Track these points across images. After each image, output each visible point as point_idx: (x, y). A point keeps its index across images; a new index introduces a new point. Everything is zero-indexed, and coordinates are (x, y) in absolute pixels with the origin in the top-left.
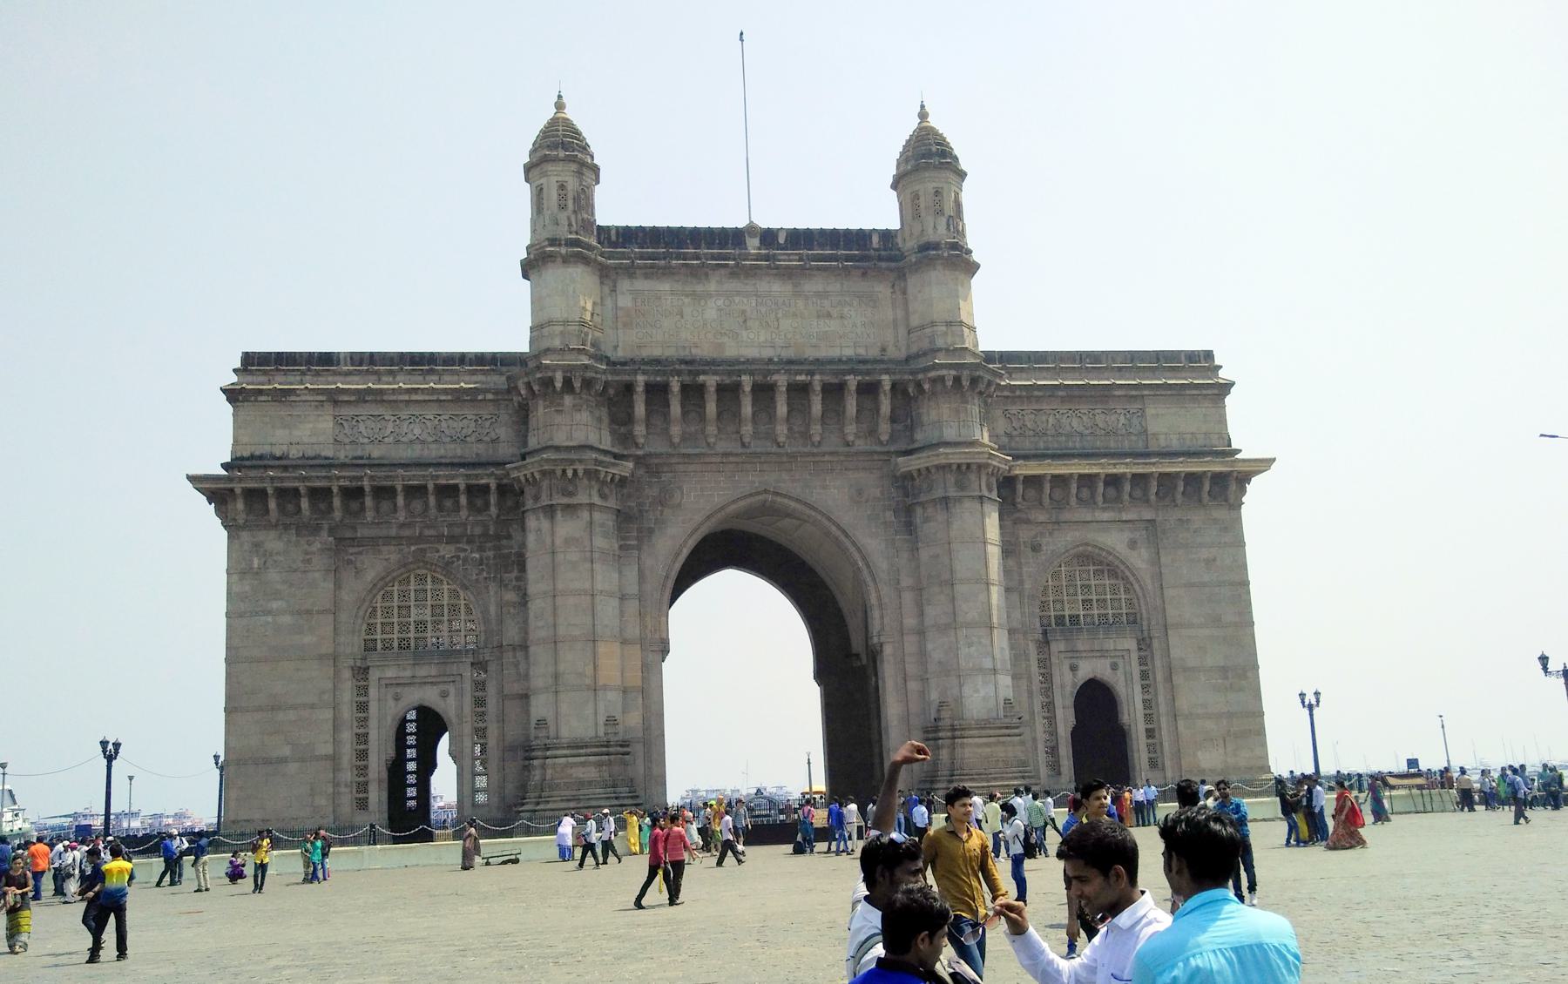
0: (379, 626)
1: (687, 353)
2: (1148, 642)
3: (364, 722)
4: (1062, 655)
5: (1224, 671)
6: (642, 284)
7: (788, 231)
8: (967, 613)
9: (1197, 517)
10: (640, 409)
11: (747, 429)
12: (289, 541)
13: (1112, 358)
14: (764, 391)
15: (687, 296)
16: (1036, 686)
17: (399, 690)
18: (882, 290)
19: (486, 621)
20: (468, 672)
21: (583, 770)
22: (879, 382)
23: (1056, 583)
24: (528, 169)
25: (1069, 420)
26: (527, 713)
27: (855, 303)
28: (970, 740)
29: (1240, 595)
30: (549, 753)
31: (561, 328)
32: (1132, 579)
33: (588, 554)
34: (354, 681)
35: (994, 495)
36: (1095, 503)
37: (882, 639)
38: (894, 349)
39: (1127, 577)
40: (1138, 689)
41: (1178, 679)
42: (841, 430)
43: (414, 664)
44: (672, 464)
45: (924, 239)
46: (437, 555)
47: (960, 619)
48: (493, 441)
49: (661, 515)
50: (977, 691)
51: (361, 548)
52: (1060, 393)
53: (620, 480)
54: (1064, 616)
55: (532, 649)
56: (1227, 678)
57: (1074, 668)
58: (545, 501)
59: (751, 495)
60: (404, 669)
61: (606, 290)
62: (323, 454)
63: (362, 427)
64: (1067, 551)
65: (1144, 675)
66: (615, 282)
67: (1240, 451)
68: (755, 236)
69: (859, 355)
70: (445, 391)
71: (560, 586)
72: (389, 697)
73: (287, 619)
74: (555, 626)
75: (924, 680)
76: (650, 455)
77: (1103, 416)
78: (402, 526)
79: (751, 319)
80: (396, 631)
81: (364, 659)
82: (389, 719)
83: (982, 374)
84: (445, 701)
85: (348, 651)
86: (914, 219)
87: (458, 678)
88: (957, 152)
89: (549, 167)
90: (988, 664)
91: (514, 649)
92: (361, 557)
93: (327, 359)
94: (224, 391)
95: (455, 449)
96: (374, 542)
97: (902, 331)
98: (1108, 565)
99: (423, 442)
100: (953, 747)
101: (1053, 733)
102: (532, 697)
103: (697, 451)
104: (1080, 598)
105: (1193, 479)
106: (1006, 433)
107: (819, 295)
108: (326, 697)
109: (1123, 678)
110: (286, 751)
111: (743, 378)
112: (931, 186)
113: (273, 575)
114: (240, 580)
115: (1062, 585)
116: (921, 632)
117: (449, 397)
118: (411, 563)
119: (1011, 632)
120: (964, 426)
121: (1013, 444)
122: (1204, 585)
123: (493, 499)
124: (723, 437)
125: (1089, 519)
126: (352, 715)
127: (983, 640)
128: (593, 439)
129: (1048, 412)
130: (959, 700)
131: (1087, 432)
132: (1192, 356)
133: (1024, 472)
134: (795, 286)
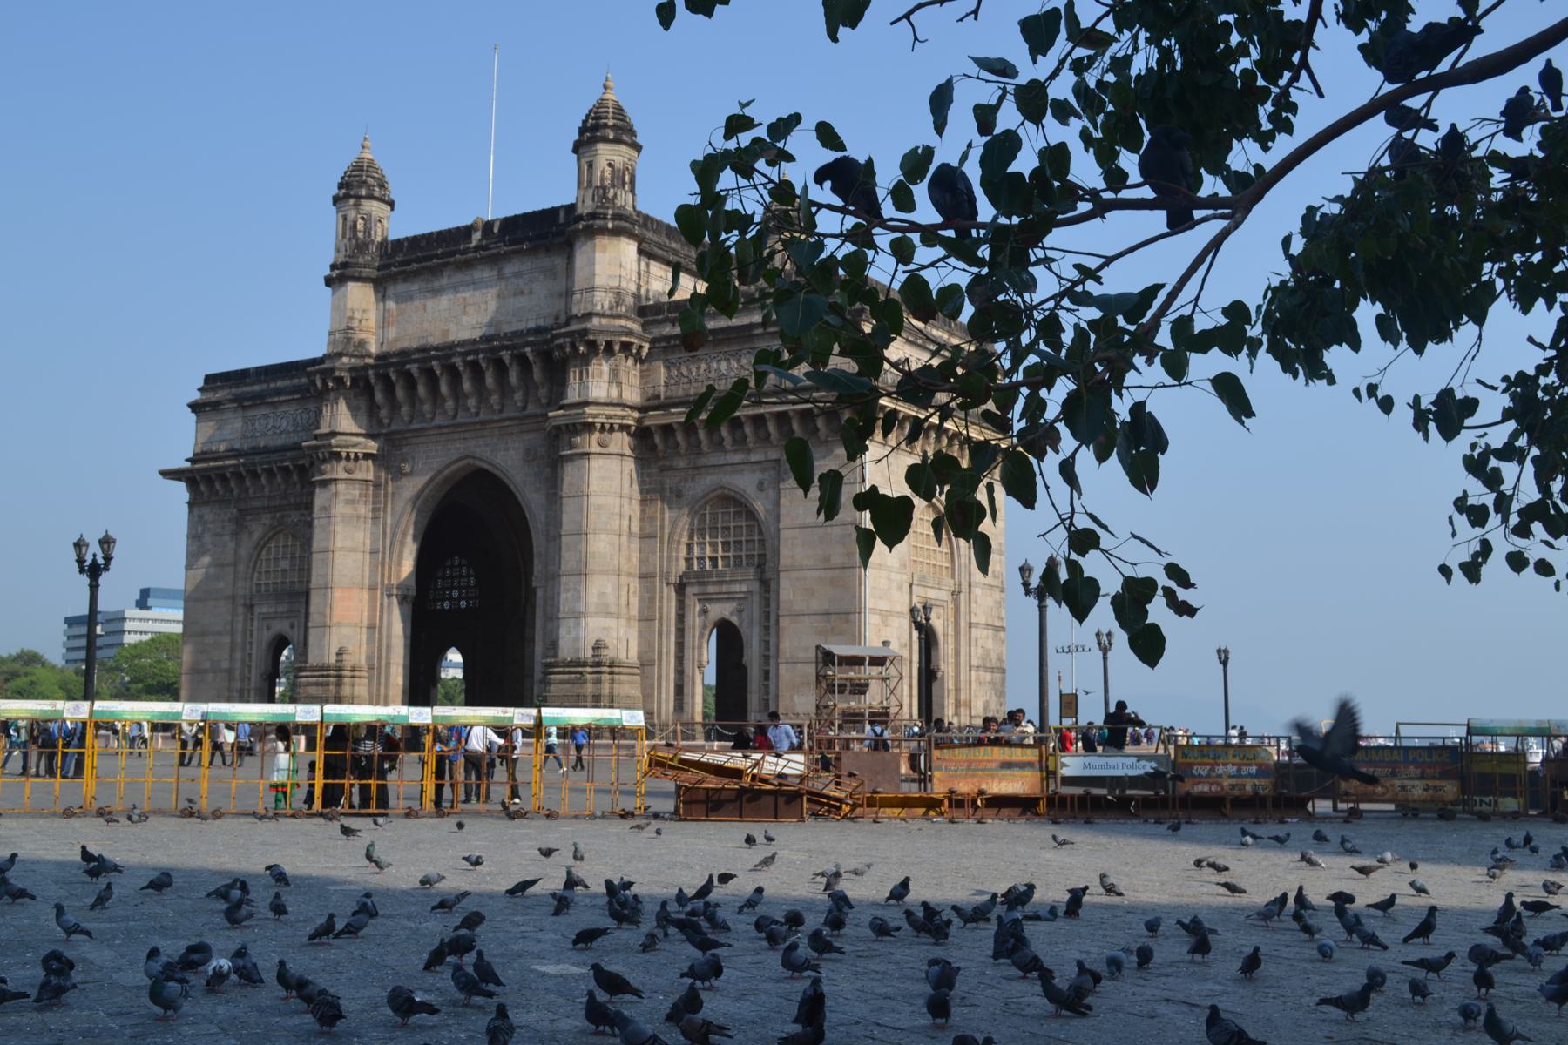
1: (422, 342)
10: (379, 397)
18: (559, 262)
21: (314, 688)
22: (524, 354)
27: (541, 278)
56: (829, 621)
57: (704, 612)
59: (457, 461)
61: (380, 295)
64: (707, 495)
76: (398, 432)
82: (264, 645)
110: (207, 665)
113: (207, 539)
121: (669, 393)
134: (500, 270)
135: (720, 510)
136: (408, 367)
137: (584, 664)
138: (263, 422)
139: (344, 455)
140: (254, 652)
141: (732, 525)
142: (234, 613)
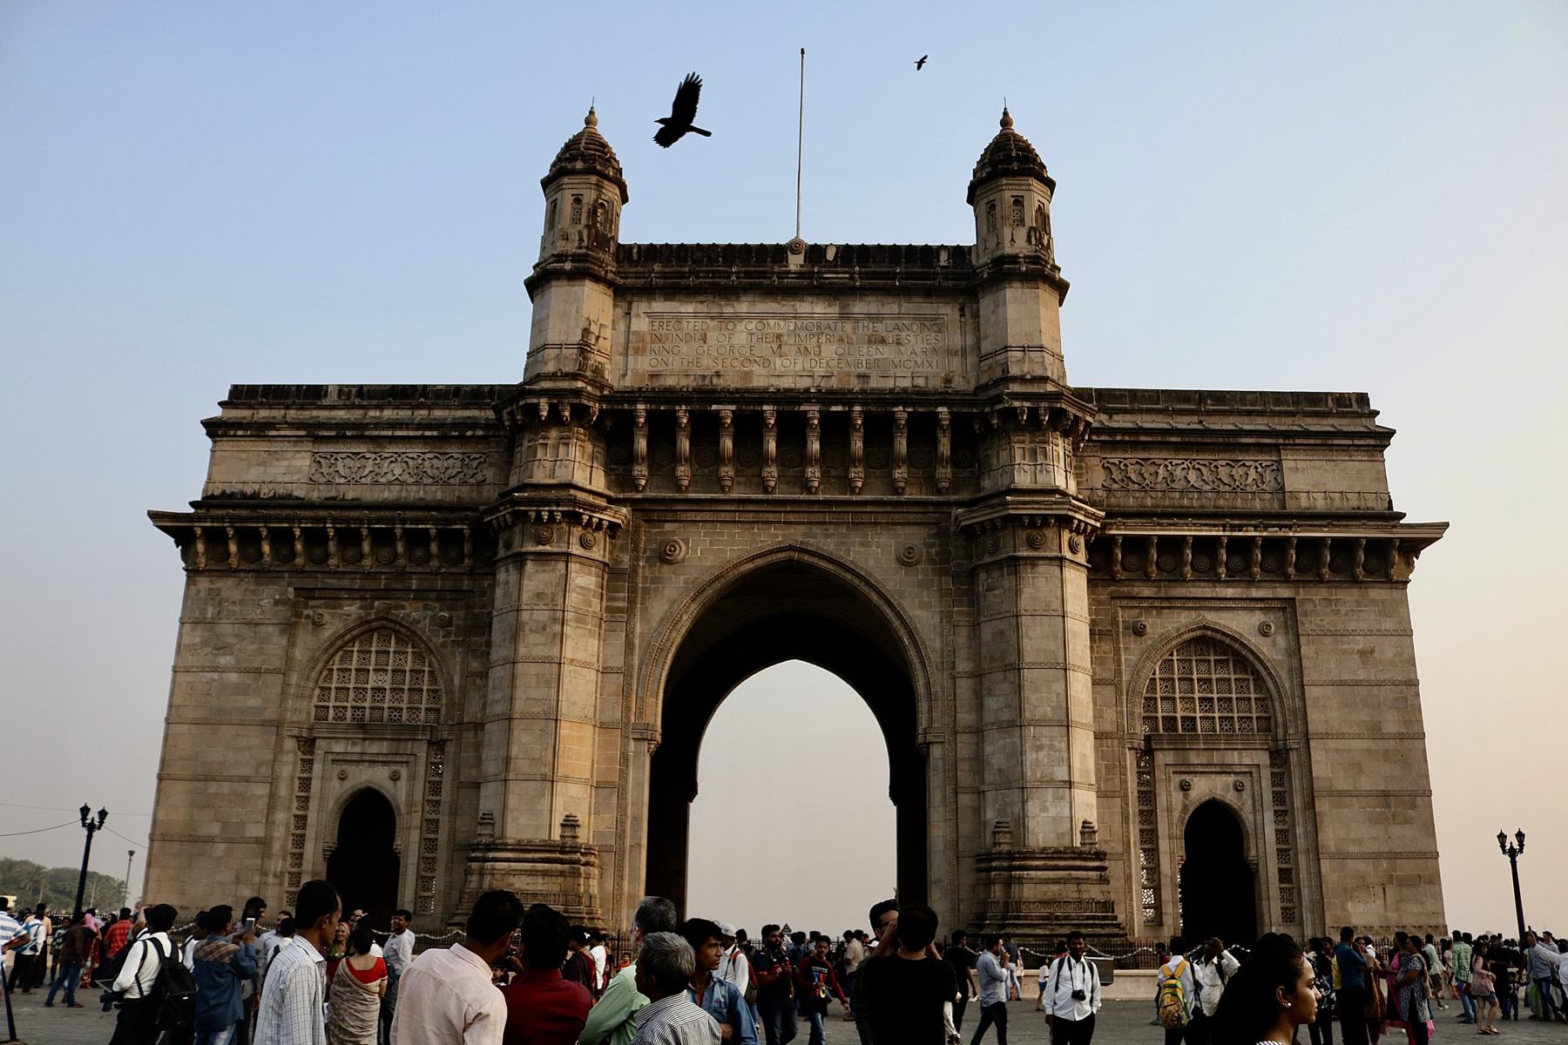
0: (333, 692)
2: (1284, 756)
3: (304, 802)
4: (1172, 769)
5: (1385, 794)
6: (659, 306)
7: (838, 247)
8: (1036, 707)
9: (1349, 596)
10: (642, 444)
11: (771, 472)
12: (246, 590)
13: (1241, 399)
14: (792, 428)
15: (712, 318)
16: (1133, 808)
17: (345, 767)
19: (450, 692)
20: (422, 750)
21: (530, 880)
23: (1166, 676)
24: (546, 183)
25: (1184, 473)
26: (478, 804)
28: (1033, 873)
29: (1406, 698)
30: (491, 855)
31: (556, 351)
32: (1264, 673)
33: (559, 614)
34: (299, 753)
35: (1081, 557)
36: (1217, 575)
37: (930, 738)
38: (961, 380)
39: (1257, 671)
40: (1269, 816)
41: (1322, 805)
42: (890, 474)
43: (364, 739)
44: (677, 510)
45: (999, 253)
46: (402, 612)
47: (1027, 715)
48: (481, 483)
49: (659, 573)
50: (1045, 809)
51: (322, 602)
52: (1173, 439)
53: (608, 527)
54: (1176, 718)
55: (487, 727)
56: (1388, 806)
57: (1185, 787)
58: (516, 549)
59: (772, 552)
60: (354, 744)
61: (620, 311)
62: (296, 493)
63: (340, 464)
65: (1279, 798)
66: (630, 303)
67: (1405, 515)
68: (794, 252)
69: (917, 387)
70: (429, 426)
71: (522, 651)
72: (335, 774)
73: (233, 677)
74: (512, 699)
75: (980, 793)
77: (1227, 469)
78: (368, 575)
79: (786, 344)
80: (351, 699)
81: (311, 729)
82: (331, 804)
83: (1064, 406)
84: (395, 785)
85: (295, 719)
86: (989, 231)
87: (412, 759)
88: (1044, 159)
89: (565, 180)
90: (1061, 773)
91: (476, 730)
92: (320, 611)
93: (313, 394)
94: (202, 422)
95: (435, 492)
96: (333, 598)
97: (971, 360)
98: (1233, 655)
99: (402, 483)
100: (1008, 883)
101: (1153, 870)
102: (483, 787)
103: (708, 496)
104: (1197, 695)
105: (1344, 548)
106: (1103, 486)
107: (871, 317)
108: (263, 769)
109: (1249, 802)
110: (215, 829)
111: (765, 408)
112: (1008, 196)
113: (225, 628)
114: (191, 631)
115: (1173, 679)
116: (978, 731)
117: (435, 433)
118: (373, 621)
119: (1099, 736)
120: (1041, 471)
121: (1113, 500)
122: (1357, 683)
123: (467, 548)
124: (742, 479)
125: (1209, 596)
126: (291, 795)
127: (1056, 744)
128: (580, 478)
129: (1157, 462)
130: (1021, 821)
131: (1208, 487)
132: (1341, 399)
133: (1123, 532)
134: (843, 307)
135: (1194, 658)
136: (714, 407)
137: (1080, 855)
138: (356, 464)
139: (586, 518)
140: (312, 816)
141: (1214, 677)
142: (278, 749)
